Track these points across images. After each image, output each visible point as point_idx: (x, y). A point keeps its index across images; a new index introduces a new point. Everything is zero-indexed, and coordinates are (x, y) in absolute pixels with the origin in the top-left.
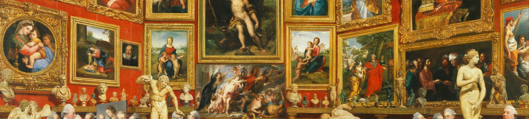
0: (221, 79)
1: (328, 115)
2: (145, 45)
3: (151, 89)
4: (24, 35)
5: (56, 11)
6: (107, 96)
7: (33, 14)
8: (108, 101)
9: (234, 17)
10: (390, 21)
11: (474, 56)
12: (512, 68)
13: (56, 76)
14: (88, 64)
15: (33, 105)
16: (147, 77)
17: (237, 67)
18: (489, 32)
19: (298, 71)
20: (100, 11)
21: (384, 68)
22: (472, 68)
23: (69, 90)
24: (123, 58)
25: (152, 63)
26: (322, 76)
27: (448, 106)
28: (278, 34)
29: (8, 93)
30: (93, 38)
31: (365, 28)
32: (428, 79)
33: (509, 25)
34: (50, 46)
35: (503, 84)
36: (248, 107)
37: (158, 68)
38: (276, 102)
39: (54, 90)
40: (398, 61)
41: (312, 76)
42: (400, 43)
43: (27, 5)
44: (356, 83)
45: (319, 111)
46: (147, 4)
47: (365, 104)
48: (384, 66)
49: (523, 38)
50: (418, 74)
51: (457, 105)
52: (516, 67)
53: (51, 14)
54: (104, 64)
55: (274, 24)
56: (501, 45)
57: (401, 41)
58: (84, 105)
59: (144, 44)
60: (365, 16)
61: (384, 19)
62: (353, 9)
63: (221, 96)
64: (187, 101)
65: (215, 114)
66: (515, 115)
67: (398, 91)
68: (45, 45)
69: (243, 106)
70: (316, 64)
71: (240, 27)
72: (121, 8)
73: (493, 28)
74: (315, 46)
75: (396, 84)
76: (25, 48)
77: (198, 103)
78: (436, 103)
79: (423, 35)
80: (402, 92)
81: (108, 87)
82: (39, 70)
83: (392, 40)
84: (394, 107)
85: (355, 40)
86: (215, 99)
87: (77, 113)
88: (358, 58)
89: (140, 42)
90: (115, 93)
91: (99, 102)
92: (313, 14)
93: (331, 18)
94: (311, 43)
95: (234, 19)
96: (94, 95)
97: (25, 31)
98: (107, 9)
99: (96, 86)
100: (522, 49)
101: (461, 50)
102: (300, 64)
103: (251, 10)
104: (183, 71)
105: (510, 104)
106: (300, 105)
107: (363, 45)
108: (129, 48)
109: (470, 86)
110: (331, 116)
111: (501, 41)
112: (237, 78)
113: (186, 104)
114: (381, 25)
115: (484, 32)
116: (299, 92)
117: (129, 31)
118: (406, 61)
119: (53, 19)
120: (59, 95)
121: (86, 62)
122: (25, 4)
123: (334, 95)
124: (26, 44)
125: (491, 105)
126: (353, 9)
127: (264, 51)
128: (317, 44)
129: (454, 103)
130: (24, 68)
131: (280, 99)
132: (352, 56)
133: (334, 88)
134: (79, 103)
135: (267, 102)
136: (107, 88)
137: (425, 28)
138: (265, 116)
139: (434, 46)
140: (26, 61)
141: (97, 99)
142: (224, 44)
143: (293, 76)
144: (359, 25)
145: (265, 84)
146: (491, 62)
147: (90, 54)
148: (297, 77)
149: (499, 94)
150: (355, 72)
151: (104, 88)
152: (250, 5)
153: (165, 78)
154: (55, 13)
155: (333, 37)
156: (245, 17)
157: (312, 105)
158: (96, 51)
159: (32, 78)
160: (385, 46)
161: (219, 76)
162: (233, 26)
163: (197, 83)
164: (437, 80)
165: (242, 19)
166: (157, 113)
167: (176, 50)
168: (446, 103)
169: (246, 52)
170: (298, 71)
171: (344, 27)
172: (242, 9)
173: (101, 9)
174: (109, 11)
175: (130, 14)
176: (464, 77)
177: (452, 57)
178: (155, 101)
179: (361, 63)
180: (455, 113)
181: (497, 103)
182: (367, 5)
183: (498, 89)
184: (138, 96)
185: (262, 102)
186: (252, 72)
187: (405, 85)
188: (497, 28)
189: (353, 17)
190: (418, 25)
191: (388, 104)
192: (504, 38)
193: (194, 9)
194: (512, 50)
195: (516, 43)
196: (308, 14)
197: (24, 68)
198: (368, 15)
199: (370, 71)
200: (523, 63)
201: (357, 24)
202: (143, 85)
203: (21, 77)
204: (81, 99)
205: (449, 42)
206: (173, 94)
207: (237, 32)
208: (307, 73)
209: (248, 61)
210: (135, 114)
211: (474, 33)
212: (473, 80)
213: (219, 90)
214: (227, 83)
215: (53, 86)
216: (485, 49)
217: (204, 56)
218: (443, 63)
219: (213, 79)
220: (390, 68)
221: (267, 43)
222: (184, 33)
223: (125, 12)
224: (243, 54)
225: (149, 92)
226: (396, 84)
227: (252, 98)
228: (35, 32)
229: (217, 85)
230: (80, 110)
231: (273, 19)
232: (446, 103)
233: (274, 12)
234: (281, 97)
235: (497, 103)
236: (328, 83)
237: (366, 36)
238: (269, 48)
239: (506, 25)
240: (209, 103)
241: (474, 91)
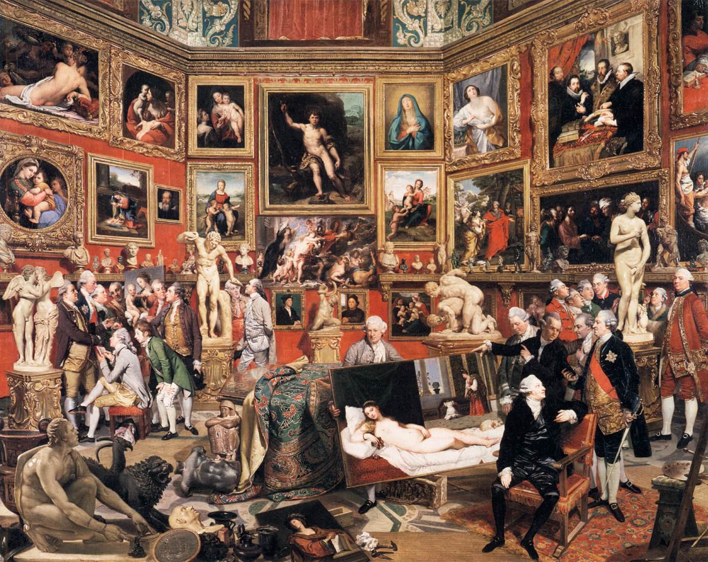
0: (291, 236)
1: (436, 284)
2: (188, 191)
3: (196, 250)
4: (26, 178)
5: (67, 147)
6: (138, 259)
7: (37, 150)
8: (140, 267)
9: (307, 153)
10: (519, 156)
11: (635, 202)
12: (687, 217)
13: (69, 233)
14: (112, 216)
15: (40, 272)
16: (192, 235)
17: (311, 219)
18: (655, 168)
19: (393, 226)
20: (128, 145)
21: (511, 220)
22: (632, 218)
23: (87, 252)
24: (159, 208)
25: (198, 216)
26: (427, 231)
27: (599, 270)
28: (367, 174)
29: (8, 256)
30: (120, 183)
31: (485, 165)
32: (570, 234)
33: (682, 159)
34: (61, 193)
35: (674, 239)
36: (327, 273)
37: (205, 222)
38: (365, 267)
39: (67, 252)
40: (530, 210)
41: (412, 232)
42: (532, 186)
43: (29, 139)
44: (472, 241)
45: (423, 278)
46: (190, 136)
47: (484, 269)
48: (511, 217)
49: (701, 176)
50: (557, 228)
51: (611, 269)
52: (692, 216)
53: (61, 150)
54: (133, 218)
55: (361, 161)
56: (672, 185)
57: (534, 183)
58: (108, 272)
59: (186, 189)
60: (484, 150)
61: (510, 154)
62: (468, 141)
63: (290, 259)
64: (245, 266)
65: (283, 282)
66: (690, 282)
67: (529, 251)
68: (54, 193)
69: (320, 272)
70: (418, 216)
71: (315, 167)
72: (155, 142)
73: (660, 164)
74: (417, 191)
75: (527, 242)
76: (28, 196)
77: (261, 269)
78: (583, 266)
79: (564, 174)
80: (535, 252)
81: (140, 247)
82: (47, 225)
83: (522, 182)
84: (524, 272)
85: (471, 182)
86: (282, 264)
87: (98, 283)
88: (474, 206)
89: (181, 187)
90: (149, 256)
91: (127, 268)
92: (413, 148)
93: (438, 153)
94: (412, 187)
95: (307, 156)
96: (121, 257)
97: (27, 173)
98: (137, 142)
99: (123, 246)
100: (700, 191)
101: (616, 194)
102: (396, 216)
103: (329, 143)
104: (239, 226)
105: (683, 267)
106: (396, 271)
107: (481, 189)
108: (166, 195)
109: (628, 243)
110: (439, 285)
111: (672, 180)
112: (312, 235)
113: (244, 270)
114: (506, 161)
115: (647, 169)
116: (395, 253)
117: (166, 172)
118: (541, 210)
119: (64, 156)
120: (74, 258)
121: (110, 215)
122: (26, 137)
123: (442, 257)
124: (28, 190)
125: (658, 268)
126: (468, 141)
127: (348, 198)
128: (419, 189)
129: (607, 266)
130: (26, 223)
131: (370, 263)
132: (467, 203)
133: (442, 248)
134: (101, 270)
135: (353, 266)
136: (138, 249)
137: (567, 164)
138: (349, 285)
139: (579, 188)
140: (29, 213)
141: (125, 263)
142: (293, 189)
143: (388, 231)
144: (477, 161)
145: (349, 243)
146: (657, 209)
147: (114, 204)
148: (392, 234)
149: (668, 253)
150: (471, 226)
151: (134, 249)
152: (329, 137)
153: (215, 235)
154: (67, 149)
155: (440, 179)
156: (321, 153)
157: (413, 271)
158: (123, 200)
159: (37, 236)
160: (512, 189)
161: (287, 232)
162: (306, 165)
163: (259, 242)
164: (583, 236)
165: (318, 155)
166: (205, 283)
167: (229, 198)
168: (595, 266)
169: (324, 200)
170: (394, 224)
171: (456, 165)
172: (318, 142)
173: (129, 142)
174: (139, 145)
175: (167, 149)
176: (620, 230)
177: (603, 204)
178: (202, 266)
179: (479, 214)
180: (608, 280)
181: (666, 265)
182: (487, 135)
183: (667, 247)
184: (179, 260)
185: (345, 268)
186: (332, 227)
187: (539, 242)
188: (665, 163)
189: (468, 152)
190: (557, 160)
191: (516, 269)
192: (676, 177)
193: (253, 143)
194: (686, 193)
195: (692, 183)
196: (407, 148)
197: (26, 223)
198: (489, 149)
199: (492, 224)
200: (702, 211)
201: (474, 160)
202: (186, 245)
203: (22, 235)
204: (104, 264)
205: (600, 184)
206: (226, 257)
207: (310, 173)
208: (407, 227)
209: (327, 212)
210: (176, 284)
211: (634, 171)
212: (632, 234)
213: (287, 252)
214: (299, 242)
215: (65, 247)
216: (650, 192)
217: (268, 205)
218: (592, 212)
219: (280, 236)
220: (519, 220)
221: (352, 187)
222: (241, 174)
223: (160, 147)
224: (320, 203)
225: (194, 254)
226: (527, 242)
227: (331, 262)
228: (40, 175)
229: (285, 245)
230: (102, 278)
231: (360, 155)
232: (595, 266)
233: (361, 144)
234: (371, 260)
235: (666, 265)
236: (434, 240)
237: (486, 177)
238: (355, 195)
239: (679, 158)
240: (275, 268)
241: (634, 250)
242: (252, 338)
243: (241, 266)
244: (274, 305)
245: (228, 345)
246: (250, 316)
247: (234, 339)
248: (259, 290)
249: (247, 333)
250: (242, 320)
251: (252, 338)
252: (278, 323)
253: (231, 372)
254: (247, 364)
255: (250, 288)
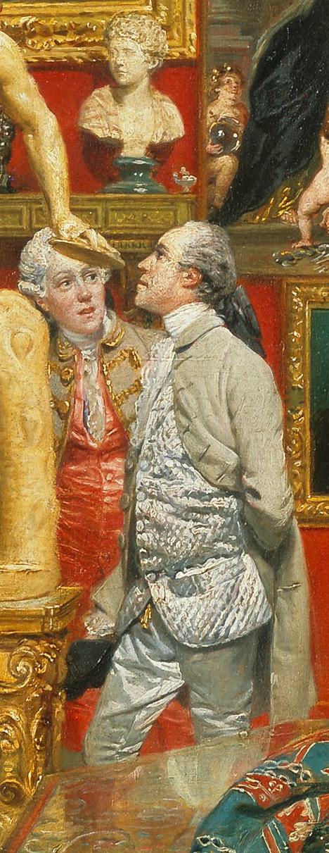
64: (134, 151)
77: (225, 164)
113: (130, 169)
242: (170, 569)
243: (117, 146)
244: (299, 378)
245: (36, 606)
246: (159, 438)
247: (66, 573)
248: (210, 288)
249: (146, 537)
250: (116, 465)
251: (170, 569)
252: (321, 484)
253: (49, 767)
254: (143, 721)
255: (162, 276)
